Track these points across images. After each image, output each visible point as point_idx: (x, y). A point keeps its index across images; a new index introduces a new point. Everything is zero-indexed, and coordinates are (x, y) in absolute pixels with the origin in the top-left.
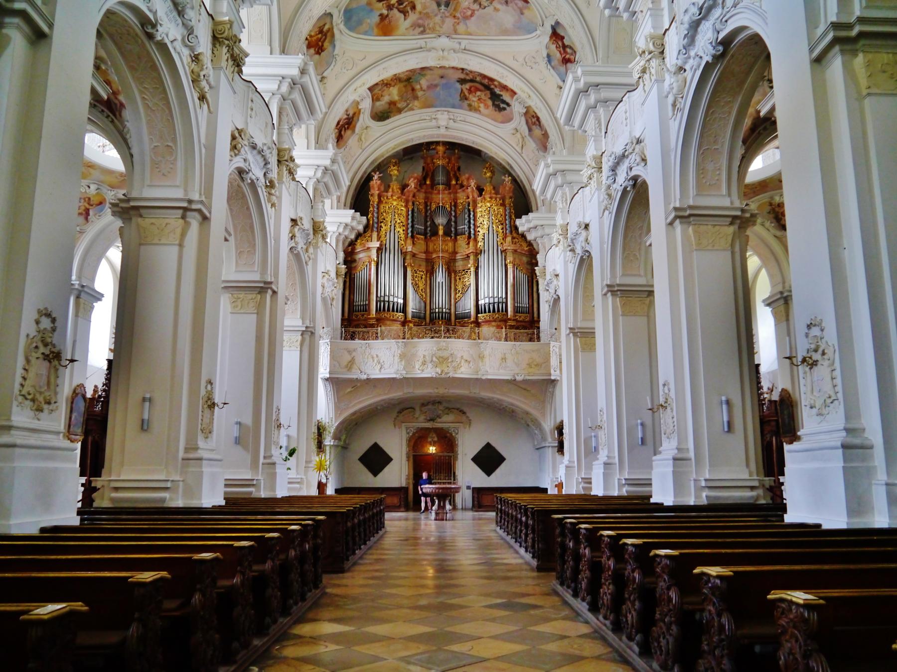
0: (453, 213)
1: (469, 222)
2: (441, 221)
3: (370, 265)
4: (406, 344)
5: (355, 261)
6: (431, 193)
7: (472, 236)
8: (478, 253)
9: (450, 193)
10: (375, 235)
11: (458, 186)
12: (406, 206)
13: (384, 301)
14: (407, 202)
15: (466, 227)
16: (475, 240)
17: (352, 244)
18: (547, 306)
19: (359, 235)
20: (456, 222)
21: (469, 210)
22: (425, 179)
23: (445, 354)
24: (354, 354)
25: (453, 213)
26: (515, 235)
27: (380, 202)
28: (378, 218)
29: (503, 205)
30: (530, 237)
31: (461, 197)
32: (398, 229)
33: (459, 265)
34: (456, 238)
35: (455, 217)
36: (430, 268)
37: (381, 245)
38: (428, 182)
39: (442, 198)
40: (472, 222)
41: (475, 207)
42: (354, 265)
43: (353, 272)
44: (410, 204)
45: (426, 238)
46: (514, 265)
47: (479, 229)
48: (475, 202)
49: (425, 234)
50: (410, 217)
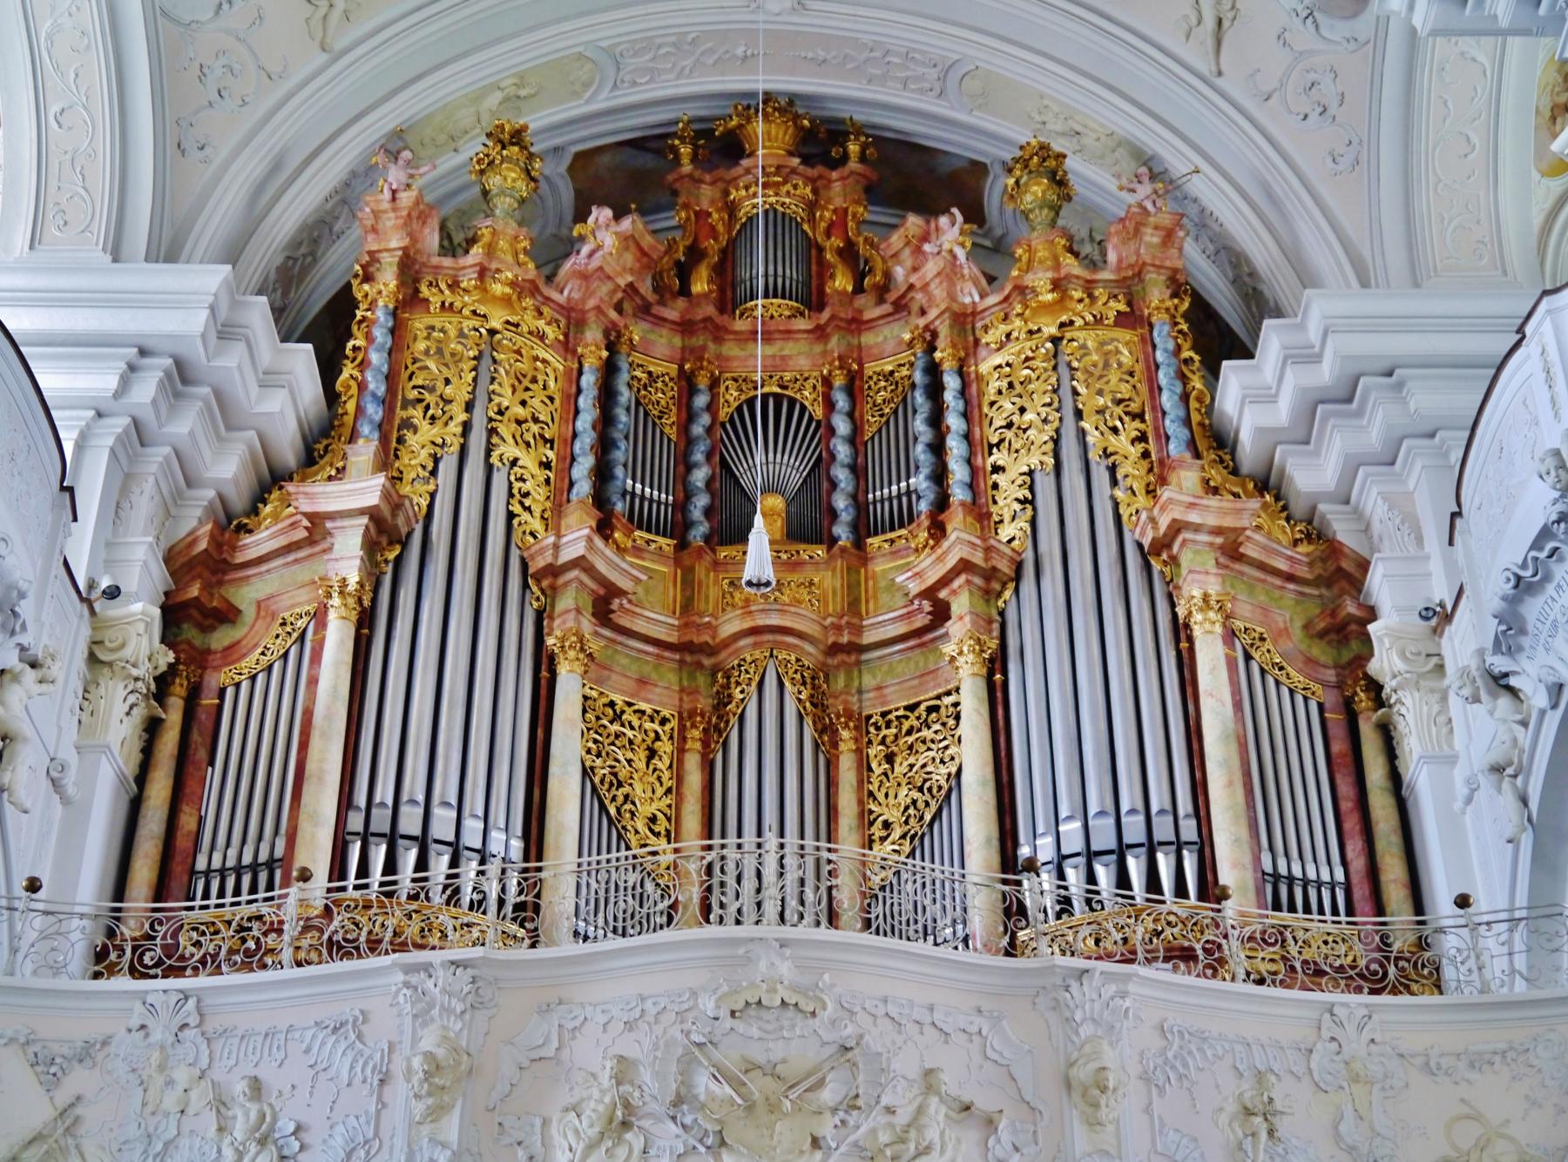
0: (842, 426)
1: (938, 448)
2: (769, 468)
3: (322, 624)
4: (480, 991)
5: (228, 615)
6: (719, 334)
7: (959, 494)
8: (997, 579)
9: (820, 333)
10: (364, 452)
11: (861, 301)
12: (567, 347)
13: (393, 838)
14: (573, 320)
15: (920, 482)
16: (981, 514)
17: (232, 524)
18: (1497, 811)
19: (271, 481)
20: (858, 470)
21: (933, 370)
22: (684, 272)
23: (798, 1047)
24: (78, 1080)
25: (842, 426)
26: (1217, 476)
27: (410, 299)
28: (391, 378)
29: (1132, 318)
30: (1310, 476)
31: (889, 346)
32: (509, 450)
33: (886, 685)
34: (859, 544)
35: (853, 440)
36: (704, 703)
37: (394, 500)
38: (700, 286)
39: (771, 353)
40: (954, 421)
41: (969, 348)
42: (221, 638)
43: (215, 679)
44: (593, 335)
45: (682, 545)
46: (1230, 635)
47: (999, 457)
48: (964, 320)
49: (679, 529)
50: (587, 402)
